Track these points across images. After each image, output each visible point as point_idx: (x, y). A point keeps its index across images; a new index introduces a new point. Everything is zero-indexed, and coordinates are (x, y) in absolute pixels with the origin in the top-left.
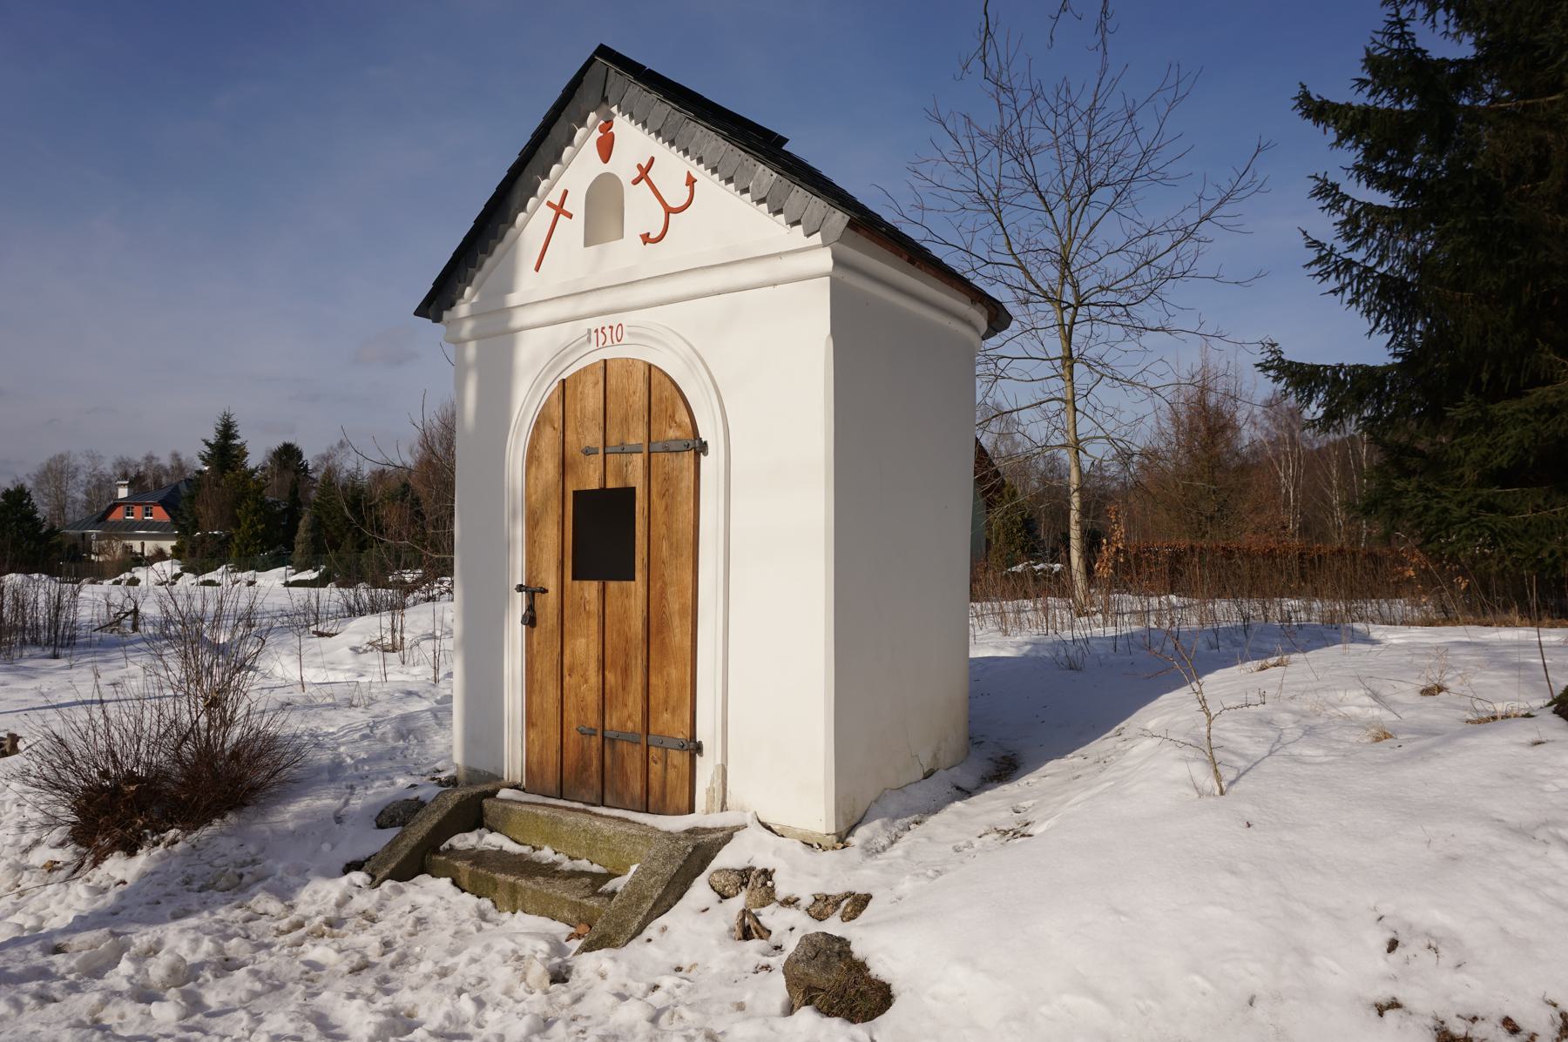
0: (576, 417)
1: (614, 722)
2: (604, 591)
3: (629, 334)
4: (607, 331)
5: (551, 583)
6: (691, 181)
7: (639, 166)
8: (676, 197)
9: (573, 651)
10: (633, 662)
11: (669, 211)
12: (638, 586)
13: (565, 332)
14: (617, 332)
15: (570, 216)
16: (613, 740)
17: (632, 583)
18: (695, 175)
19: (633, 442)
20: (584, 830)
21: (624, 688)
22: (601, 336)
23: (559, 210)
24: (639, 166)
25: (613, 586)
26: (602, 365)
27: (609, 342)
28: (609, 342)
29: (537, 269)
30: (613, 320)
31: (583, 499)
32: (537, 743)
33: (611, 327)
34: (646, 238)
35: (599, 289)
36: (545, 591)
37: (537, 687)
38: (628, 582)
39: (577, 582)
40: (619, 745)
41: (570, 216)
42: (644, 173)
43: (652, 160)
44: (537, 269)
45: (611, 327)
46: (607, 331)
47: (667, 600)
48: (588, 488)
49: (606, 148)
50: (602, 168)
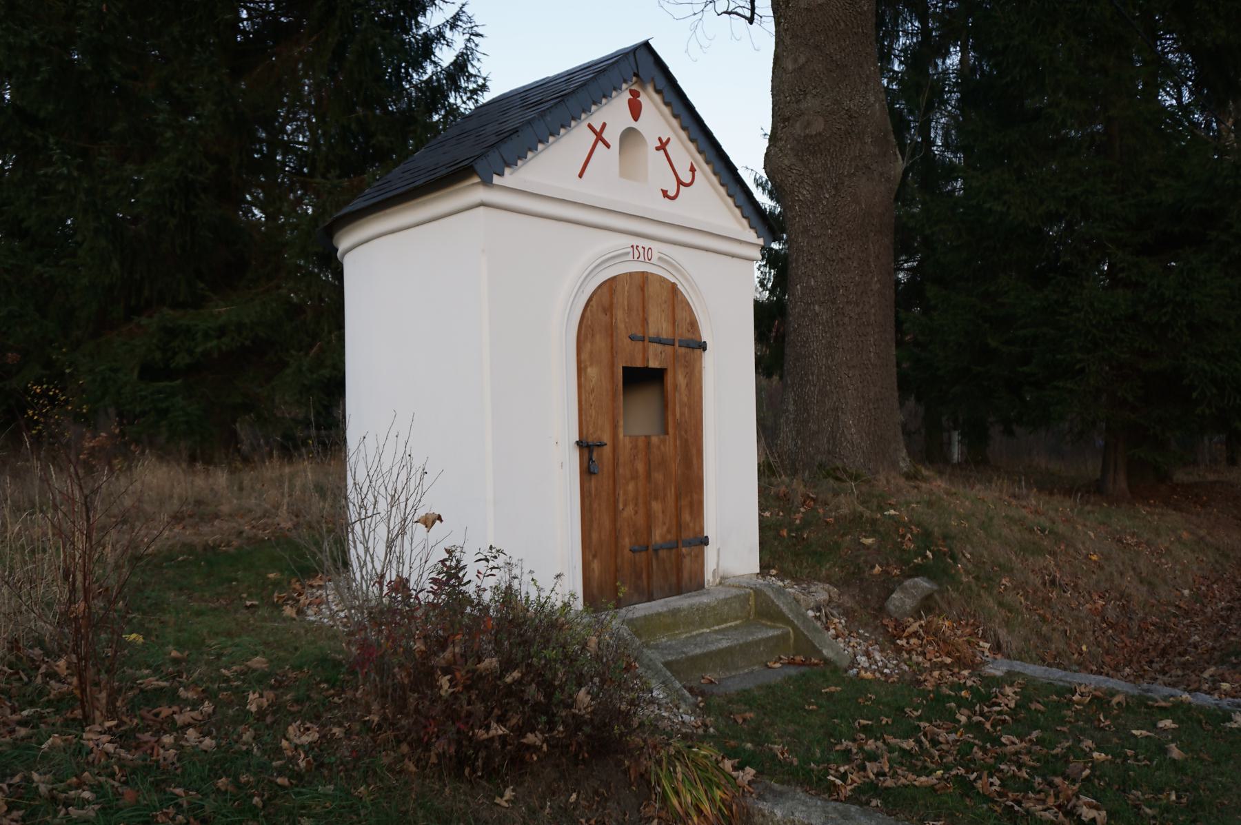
3: (660, 258)
4: (640, 249)
6: (693, 170)
7: (660, 139)
8: (686, 178)
10: (669, 492)
11: (680, 183)
14: (647, 255)
19: (665, 337)
21: (663, 512)
22: (636, 255)
23: (599, 137)
28: (641, 258)
29: (580, 176)
30: (647, 244)
44: (580, 176)
45: (632, 246)
49: (635, 110)
50: (631, 123)
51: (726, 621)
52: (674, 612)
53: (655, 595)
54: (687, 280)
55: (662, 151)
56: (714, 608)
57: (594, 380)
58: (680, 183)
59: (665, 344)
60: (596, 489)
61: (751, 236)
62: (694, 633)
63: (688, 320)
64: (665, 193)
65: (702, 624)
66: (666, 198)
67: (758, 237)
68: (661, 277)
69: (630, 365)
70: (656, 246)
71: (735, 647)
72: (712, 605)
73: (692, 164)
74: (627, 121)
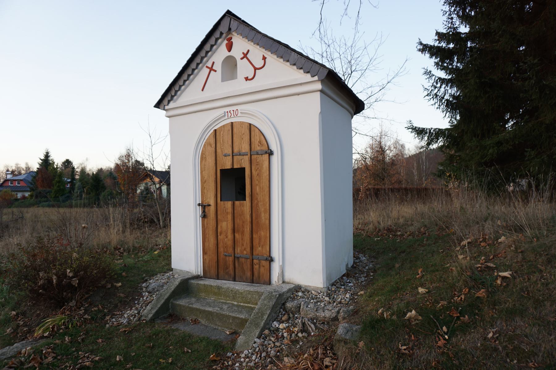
0: (220, 143)
1: (239, 251)
2: (233, 205)
3: (241, 113)
4: (232, 112)
5: (212, 202)
6: (264, 58)
7: (243, 53)
8: (259, 64)
9: (221, 227)
10: (246, 230)
11: (256, 69)
12: (247, 202)
13: (220, 112)
15: (215, 71)
16: (238, 258)
17: (245, 202)
18: (266, 56)
19: (243, 151)
20: (231, 291)
21: (242, 239)
22: (229, 114)
23: (211, 69)
24: (243, 53)
25: (237, 203)
26: (231, 124)
27: (233, 116)
28: (233, 116)
29: (203, 90)
30: (234, 108)
31: (224, 172)
32: (207, 260)
33: (233, 111)
34: (247, 79)
35: (229, 97)
36: (210, 205)
37: (207, 240)
38: (243, 201)
39: (222, 202)
40: (241, 259)
41: (215, 71)
42: (245, 56)
43: (248, 51)
44: (203, 90)
45: (233, 111)
46: (232, 112)
47: (259, 207)
48: (226, 168)
49: (230, 47)
51: (249, 303)
52: (219, 288)
53: (237, 279)
54: (259, 119)
55: (245, 59)
56: (241, 293)
57: (206, 177)
58: (256, 69)
59: (243, 155)
60: (207, 224)
61: (308, 77)
62: (228, 302)
63: (258, 140)
64: (247, 79)
65: (234, 299)
66: (248, 81)
67: (313, 76)
68: (241, 122)
69: (224, 168)
70: (239, 108)
71: (214, 312)
72: (240, 291)
73: (263, 55)
74: (226, 53)
